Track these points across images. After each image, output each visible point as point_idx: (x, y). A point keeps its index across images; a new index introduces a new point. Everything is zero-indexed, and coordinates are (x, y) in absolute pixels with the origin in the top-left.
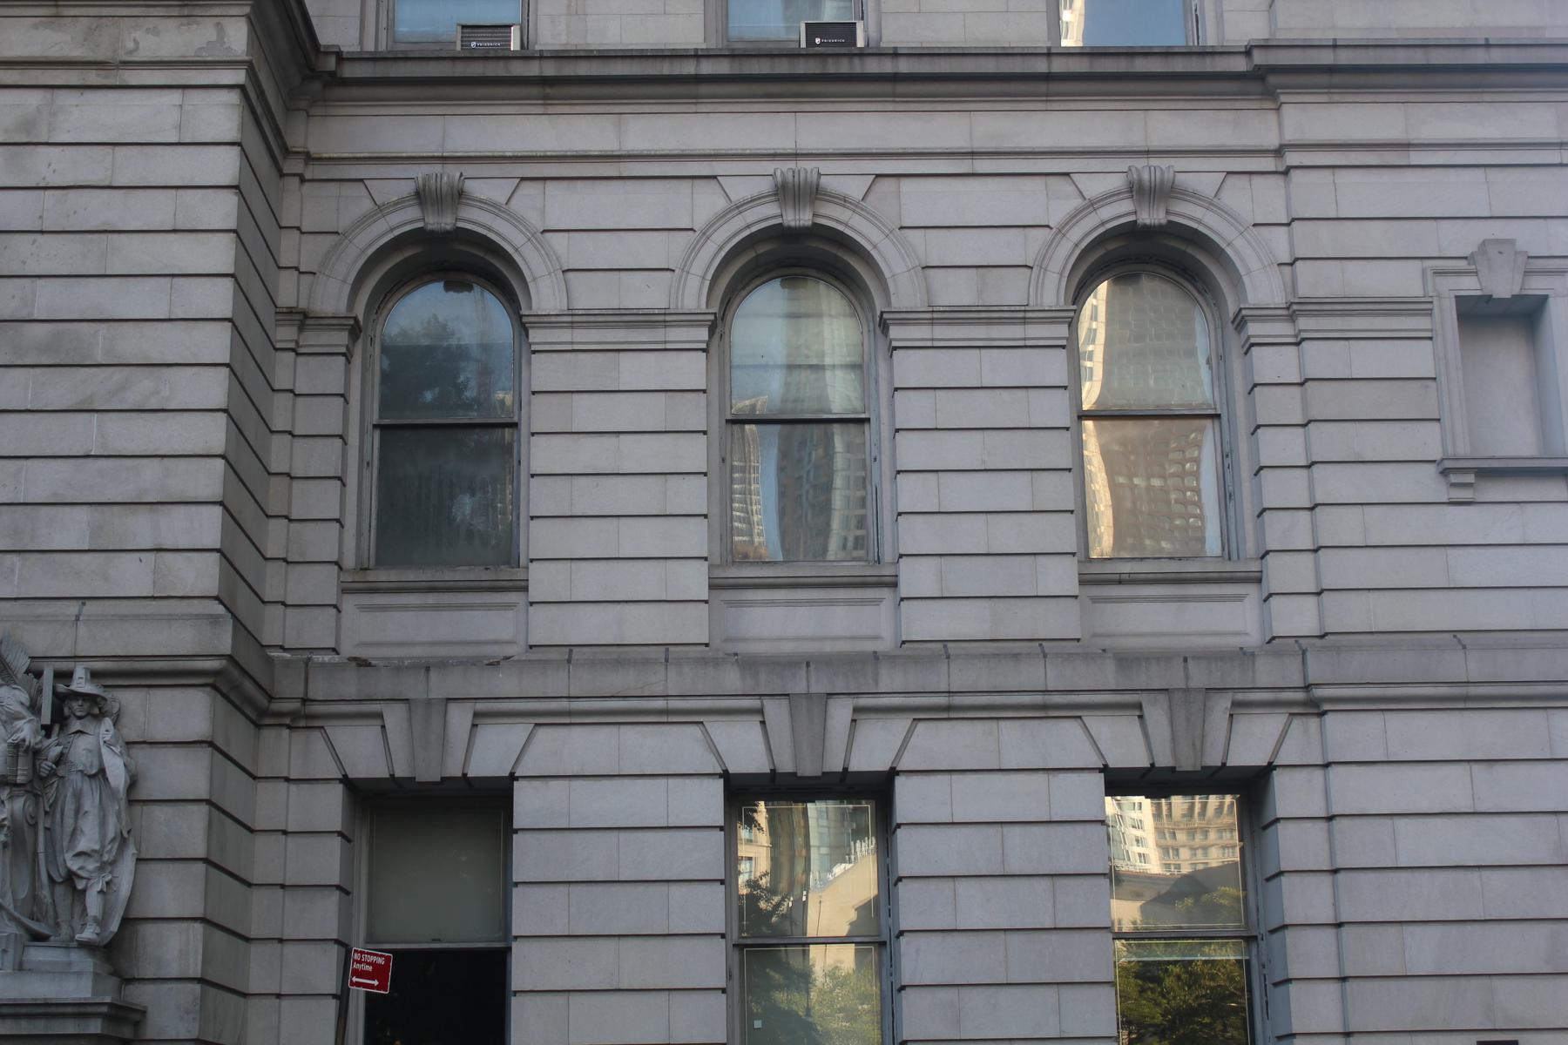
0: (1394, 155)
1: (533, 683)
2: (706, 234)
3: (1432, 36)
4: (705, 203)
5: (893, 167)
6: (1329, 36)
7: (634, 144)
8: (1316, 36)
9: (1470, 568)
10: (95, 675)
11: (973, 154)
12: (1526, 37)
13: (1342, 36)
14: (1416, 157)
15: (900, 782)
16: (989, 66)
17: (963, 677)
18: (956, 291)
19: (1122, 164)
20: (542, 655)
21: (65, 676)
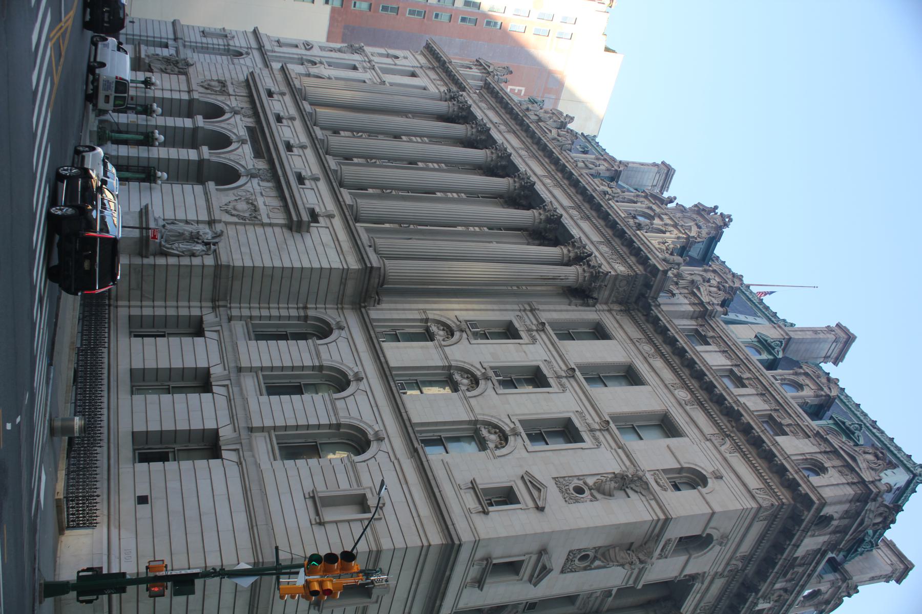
0: (403, 480)
1: (227, 339)
2: (342, 364)
3: (438, 479)
4: (351, 364)
5: (370, 394)
6: (455, 522)
7: (361, 354)
9: (286, 499)
10: (215, 251)
11: (377, 406)
12: (450, 510)
13: (457, 526)
14: (405, 487)
15: (220, 460)
16: (449, 523)
17: (238, 401)
18: (340, 404)
19: (382, 428)
20: (235, 347)
21: (214, 244)
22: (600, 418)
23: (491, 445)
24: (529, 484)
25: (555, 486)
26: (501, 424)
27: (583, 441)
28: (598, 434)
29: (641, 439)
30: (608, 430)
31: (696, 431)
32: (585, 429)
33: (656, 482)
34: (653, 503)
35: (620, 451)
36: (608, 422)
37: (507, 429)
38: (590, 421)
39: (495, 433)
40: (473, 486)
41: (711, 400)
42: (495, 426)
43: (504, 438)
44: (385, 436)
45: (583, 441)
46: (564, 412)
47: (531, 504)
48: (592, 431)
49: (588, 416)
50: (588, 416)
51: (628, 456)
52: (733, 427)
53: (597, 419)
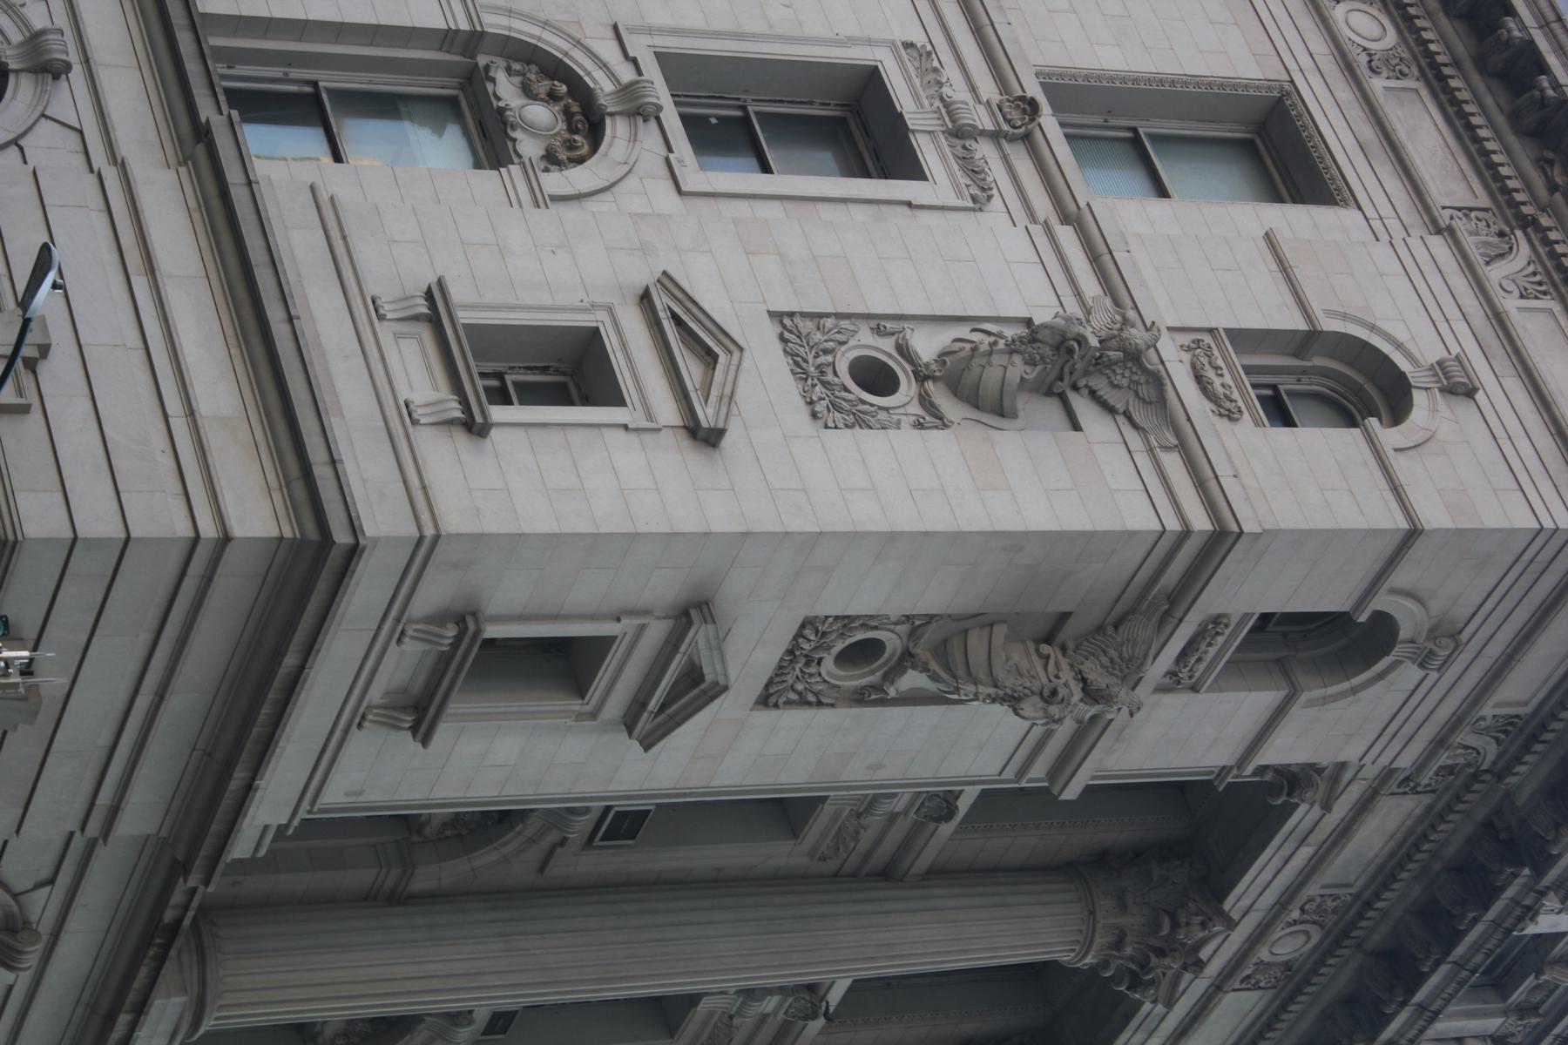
6: (343, 451)
8: (335, 425)
13: (349, 469)
22: (1003, 86)
23: (530, 148)
24: (668, 325)
25: (777, 347)
26: (580, 62)
27: (915, 171)
28: (984, 150)
29: (1162, 192)
30: (1027, 138)
31: (1395, 186)
32: (932, 124)
33: (1199, 378)
34: (1173, 464)
35: (1066, 234)
36: (1032, 107)
37: (603, 85)
38: (958, 91)
39: (553, 97)
40: (434, 311)
41: (1480, 63)
42: (555, 69)
43: (586, 123)
44: (74, 57)
45: (915, 171)
46: (851, 41)
47: (667, 411)
48: (960, 133)
49: (951, 72)
50: (951, 72)
51: (1094, 258)
52: (1553, 187)
53: (988, 89)
